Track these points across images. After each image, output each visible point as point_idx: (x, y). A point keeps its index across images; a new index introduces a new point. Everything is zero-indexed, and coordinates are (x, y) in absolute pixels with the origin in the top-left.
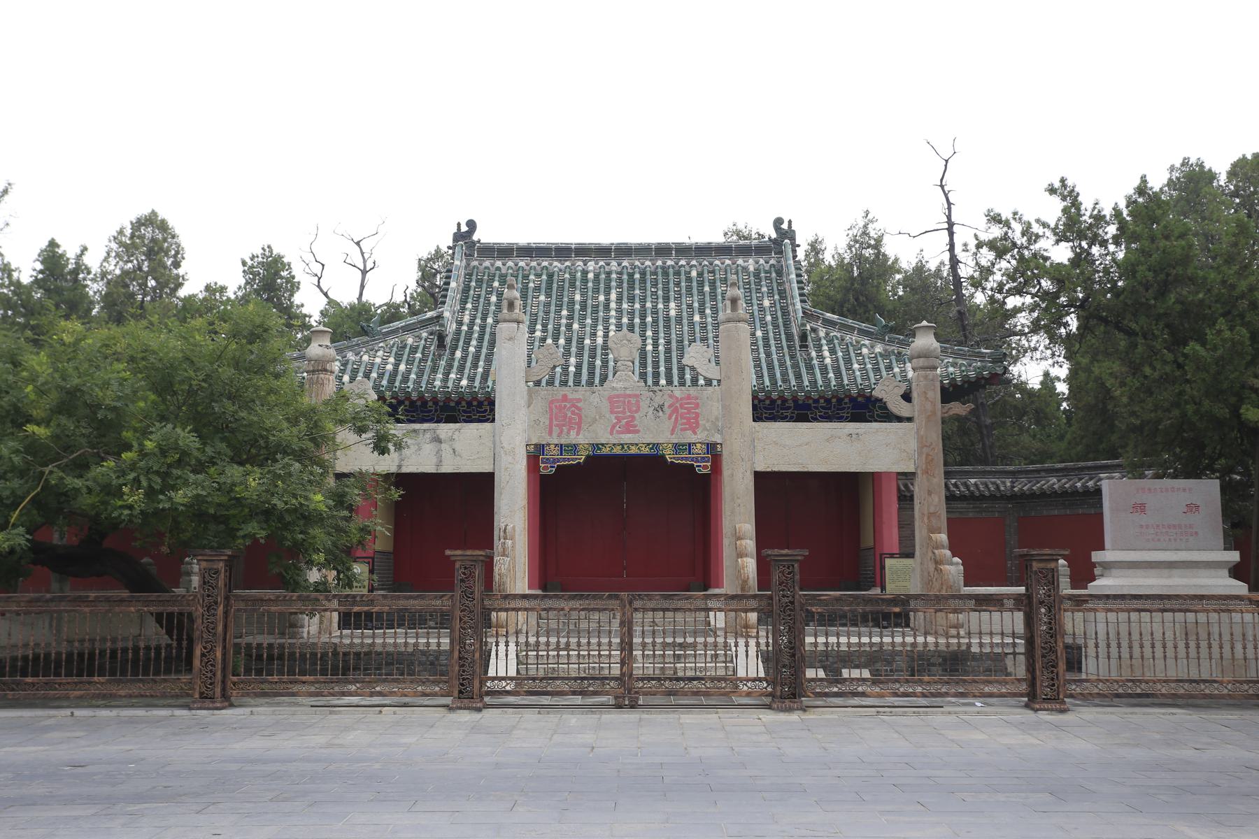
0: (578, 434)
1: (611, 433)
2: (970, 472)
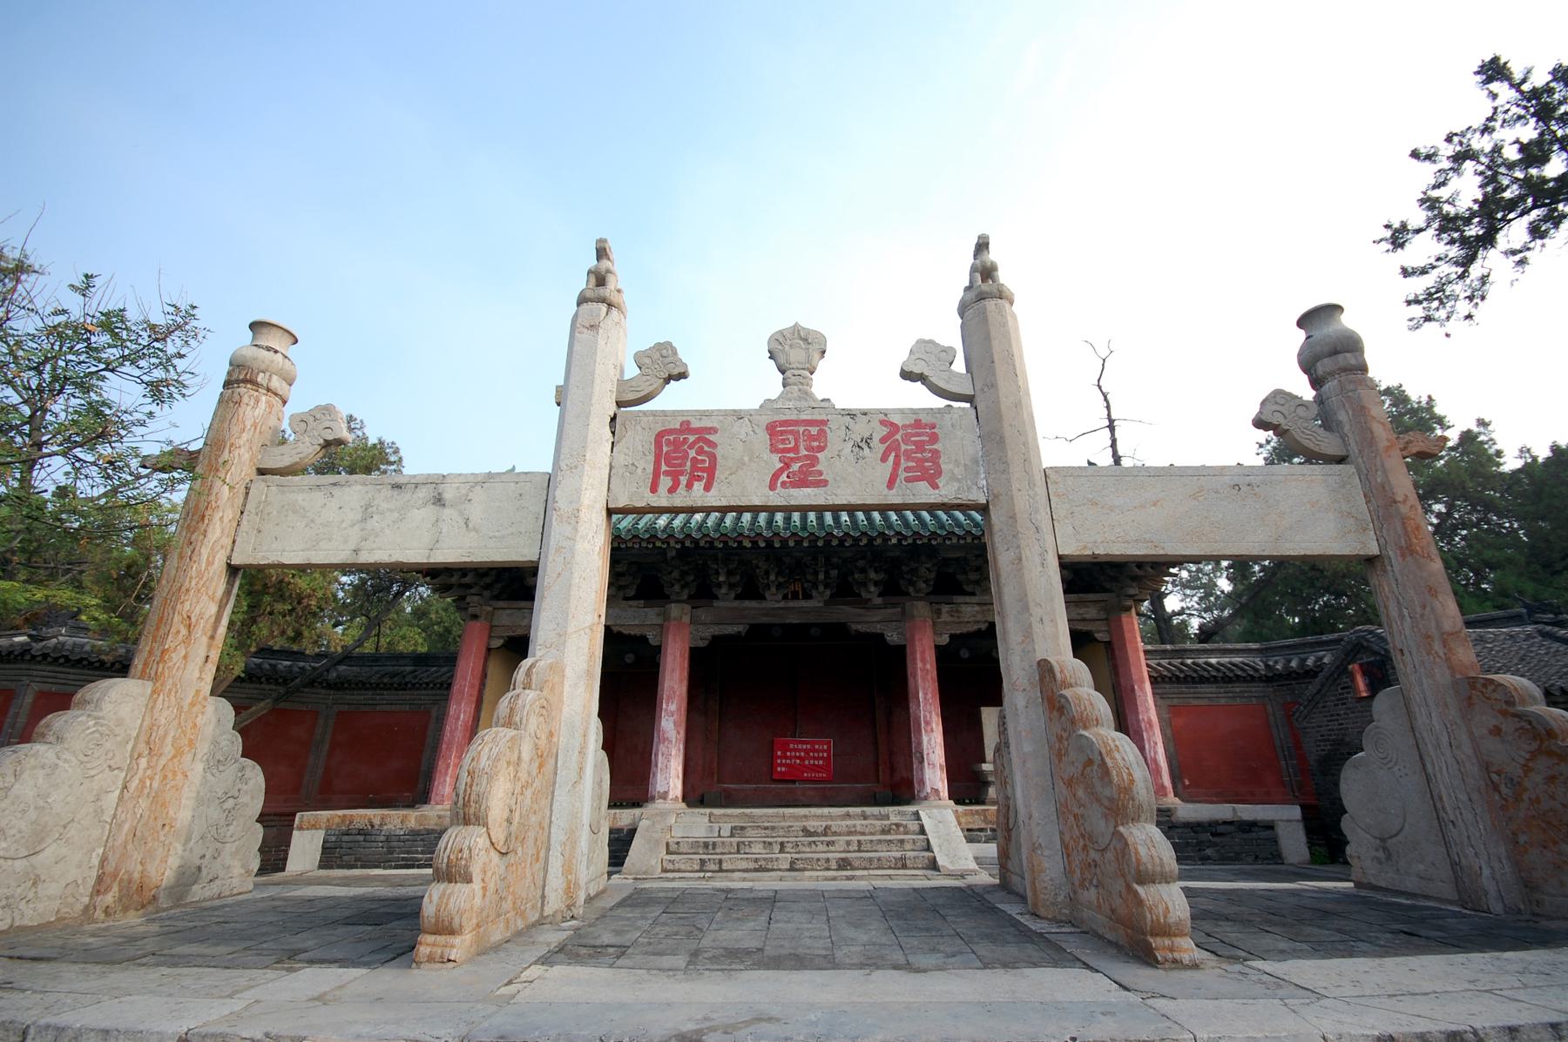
0: (707, 488)
1: (772, 487)
2: (1208, 650)
